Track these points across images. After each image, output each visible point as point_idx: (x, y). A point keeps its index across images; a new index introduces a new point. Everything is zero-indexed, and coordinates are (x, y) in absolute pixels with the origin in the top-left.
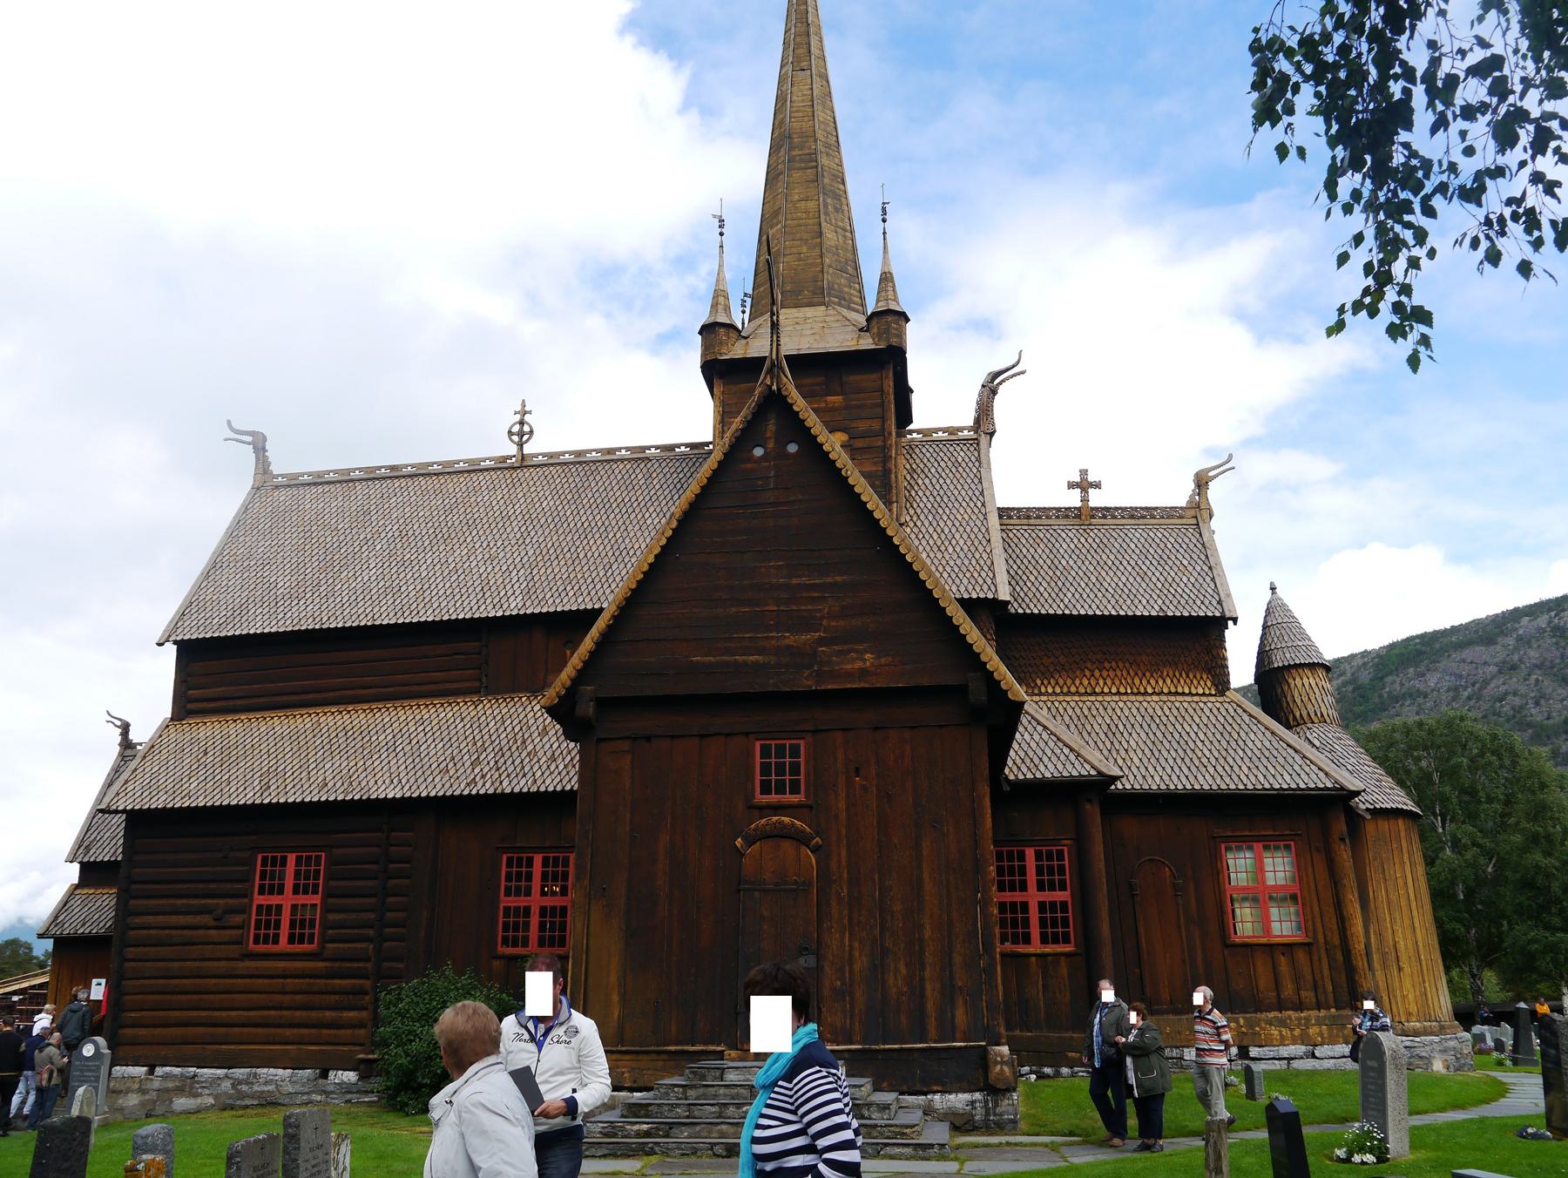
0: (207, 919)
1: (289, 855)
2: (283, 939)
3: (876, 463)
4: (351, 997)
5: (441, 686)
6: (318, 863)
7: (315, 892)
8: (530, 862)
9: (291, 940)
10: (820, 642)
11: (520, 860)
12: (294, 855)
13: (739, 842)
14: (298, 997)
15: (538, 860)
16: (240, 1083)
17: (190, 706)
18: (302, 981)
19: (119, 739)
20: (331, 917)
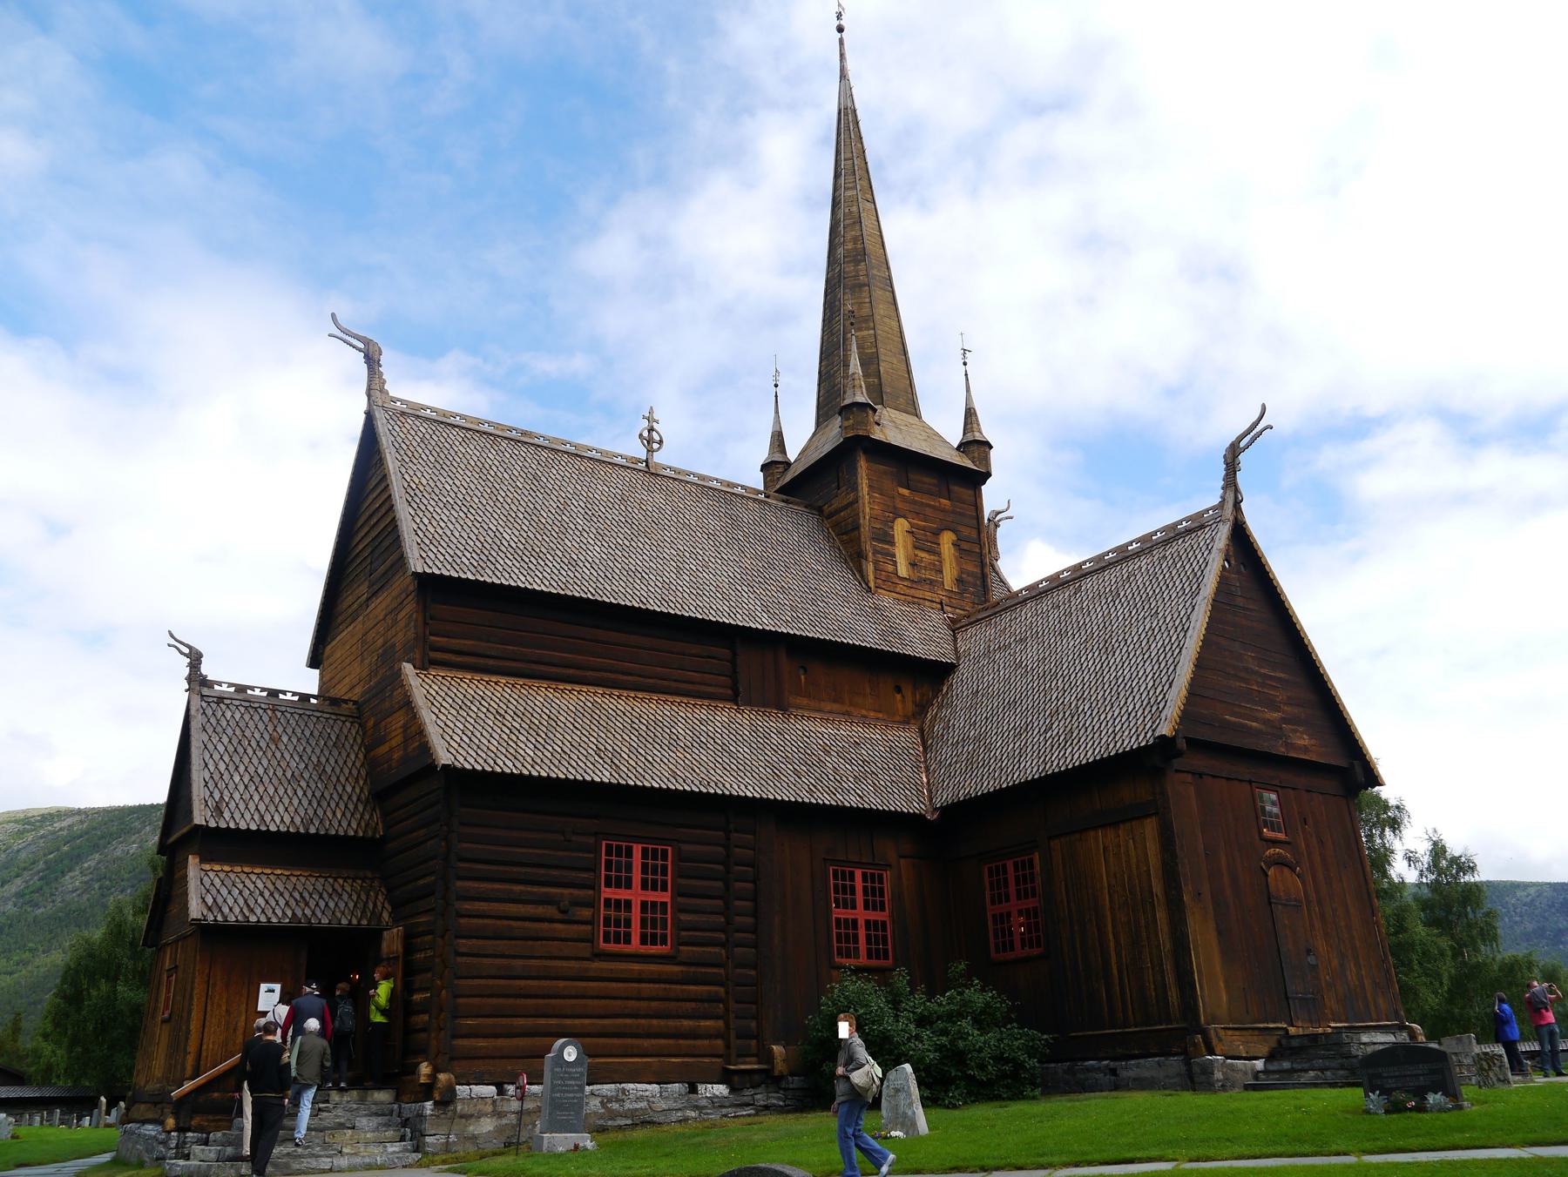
0: (551, 911)
1: (635, 846)
2: (636, 939)
3: (976, 566)
4: (706, 1005)
5: (698, 687)
6: (665, 857)
7: (664, 889)
9: (643, 941)
10: (1284, 720)
11: (843, 873)
12: (640, 846)
14: (654, 1004)
15: (858, 874)
16: (610, 1100)
17: (433, 655)
18: (657, 986)
19: (187, 671)
20: (683, 917)
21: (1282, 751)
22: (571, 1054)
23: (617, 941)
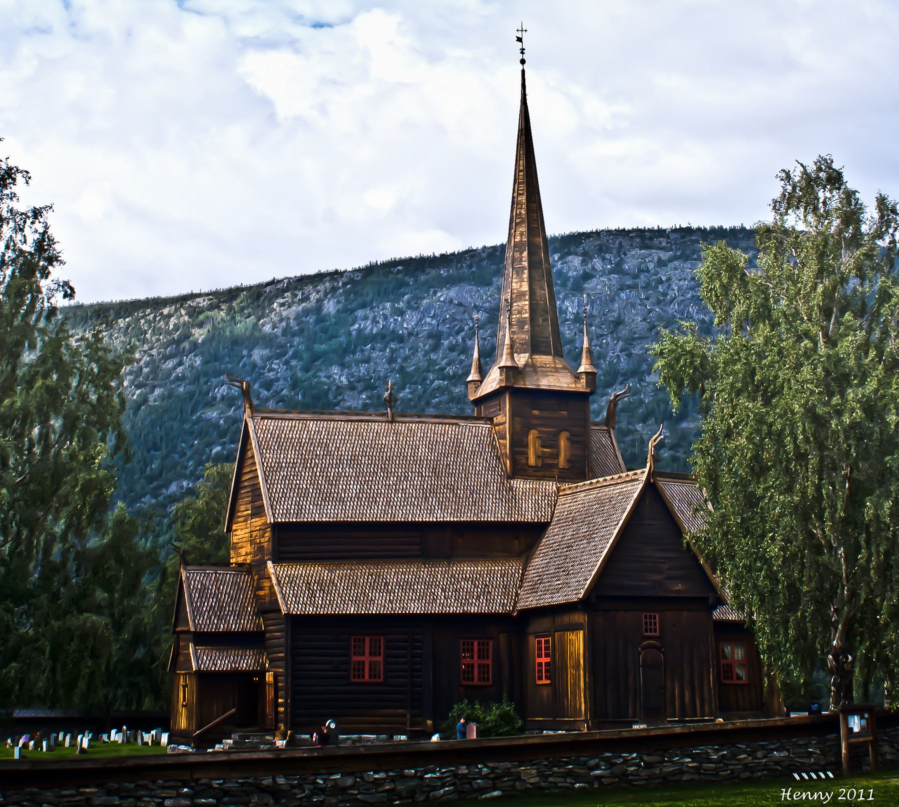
7: (380, 654)
8: (472, 644)
13: (639, 649)
21: (661, 594)
22: (333, 726)
23: (359, 677)
